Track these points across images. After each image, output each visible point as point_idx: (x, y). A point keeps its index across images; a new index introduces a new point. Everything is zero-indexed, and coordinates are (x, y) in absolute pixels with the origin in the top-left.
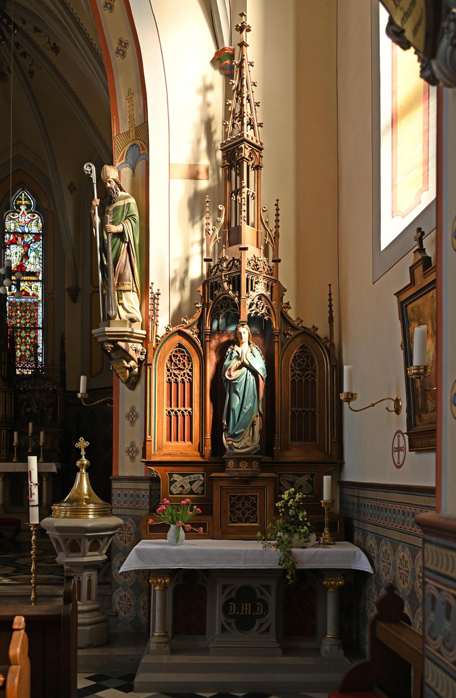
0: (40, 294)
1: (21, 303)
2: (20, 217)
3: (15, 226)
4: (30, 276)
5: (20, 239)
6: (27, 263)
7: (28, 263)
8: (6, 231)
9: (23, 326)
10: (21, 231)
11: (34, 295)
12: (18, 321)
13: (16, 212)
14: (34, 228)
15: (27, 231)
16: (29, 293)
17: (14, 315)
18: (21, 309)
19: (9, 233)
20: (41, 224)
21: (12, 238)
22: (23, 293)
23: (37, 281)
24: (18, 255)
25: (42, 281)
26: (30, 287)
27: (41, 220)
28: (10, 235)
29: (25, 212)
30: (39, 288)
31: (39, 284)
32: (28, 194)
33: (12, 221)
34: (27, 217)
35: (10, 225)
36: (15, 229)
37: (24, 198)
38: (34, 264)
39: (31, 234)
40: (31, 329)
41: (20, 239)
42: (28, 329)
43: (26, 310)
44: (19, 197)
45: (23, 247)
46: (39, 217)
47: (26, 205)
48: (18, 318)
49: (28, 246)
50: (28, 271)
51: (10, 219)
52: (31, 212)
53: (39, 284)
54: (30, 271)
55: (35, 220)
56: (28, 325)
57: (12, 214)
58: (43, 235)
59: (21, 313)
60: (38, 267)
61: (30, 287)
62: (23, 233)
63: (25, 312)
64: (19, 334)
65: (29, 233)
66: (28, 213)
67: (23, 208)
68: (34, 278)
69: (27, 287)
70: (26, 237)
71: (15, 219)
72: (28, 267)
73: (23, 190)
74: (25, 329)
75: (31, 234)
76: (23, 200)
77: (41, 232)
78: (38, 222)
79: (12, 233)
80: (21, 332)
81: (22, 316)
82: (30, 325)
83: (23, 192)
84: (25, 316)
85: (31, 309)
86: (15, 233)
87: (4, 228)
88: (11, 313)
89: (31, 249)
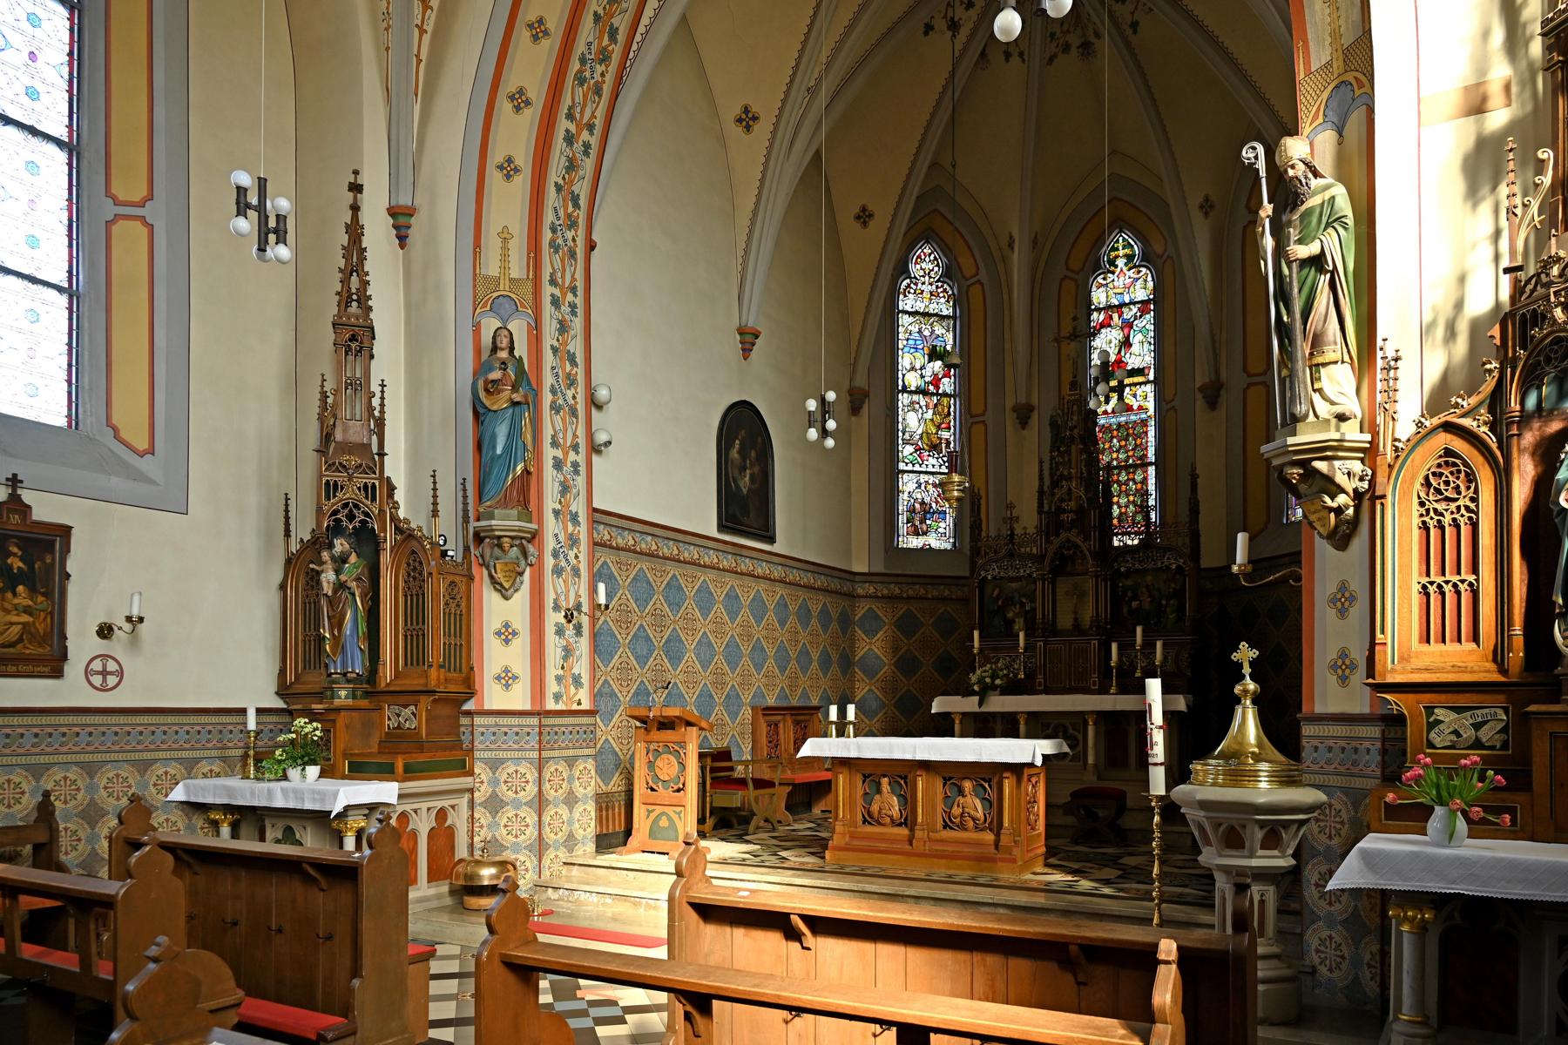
0: (1150, 405)
5: (1115, 316)
11: (1140, 408)
19: (1099, 310)
20: (1150, 284)
21: (1102, 317)
25: (1155, 382)
26: (1135, 396)
31: (1149, 388)
35: (1099, 297)
37: (1123, 245)
40: (1135, 466)
41: (1115, 316)
47: (1126, 255)
49: (1131, 327)
58: (1155, 301)
61: (1135, 396)
62: (1122, 305)
65: (1133, 303)
68: (1141, 379)
70: (1125, 310)
74: (1126, 467)
87: (1090, 302)
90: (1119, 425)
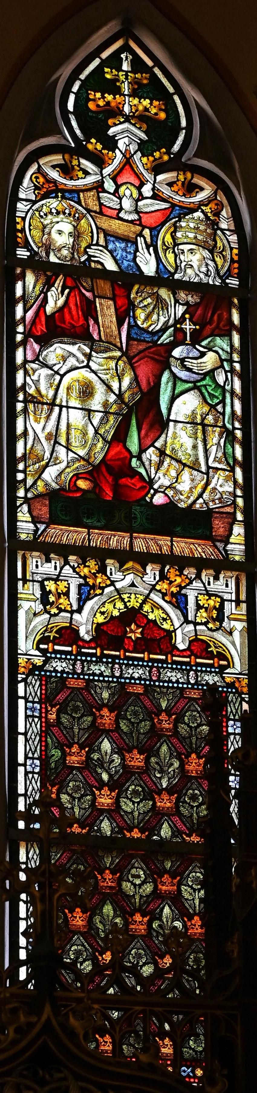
1: (122, 695)
2: (109, 185)
3: (77, 235)
4: (172, 534)
5: (107, 311)
6: (151, 454)
7: (162, 453)
8: (22, 253)
9: (136, 834)
10: (111, 266)
11: (199, 647)
12: (105, 799)
13: (81, 151)
14: (195, 259)
15: (148, 267)
16: (169, 634)
17: (74, 760)
18: (124, 726)
22: (135, 633)
23: (221, 565)
24: (96, 403)
26: (179, 601)
27: (236, 216)
28: (49, 284)
29: (140, 161)
30: (229, 608)
32: (157, 63)
33: (54, 203)
34: (147, 190)
36: (74, 248)
38: (194, 467)
39: (175, 286)
41: (107, 311)
42: (168, 855)
43: (156, 734)
44: (99, 70)
45: (130, 358)
46: (221, 197)
47: (141, 118)
48: (101, 785)
49: (163, 362)
50: (159, 499)
51: (48, 190)
52: (175, 164)
53: (226, 586)
54: (171, 506)
55: (198, 214)
56: (165, 831)
57: (57, 159)
59: (120, 750)
60: (222, 484)
61: (179, 601)
62: (126, 282)
63: (149, 751)
64: (108, 880)
65: (164, 279)
66: (157, 169)
67: (126, 135)
69: (156, 597)
71: (77, 191)
72: (162, 480)
73: (125, 32)
74: (152, 853)
75: (175, 286)
76: (126, 88)
77: (233, 282)
78: (214, 225)
79: (57, 269)
80: (121, 871)
81: (127, 772)
82: (176, 832)
83: (126, 48)
84: (147, 769)
85: (183, 729)
86: (78, 273)
88: (60, 746)
89: (175, 378)
90: (122, 691)
